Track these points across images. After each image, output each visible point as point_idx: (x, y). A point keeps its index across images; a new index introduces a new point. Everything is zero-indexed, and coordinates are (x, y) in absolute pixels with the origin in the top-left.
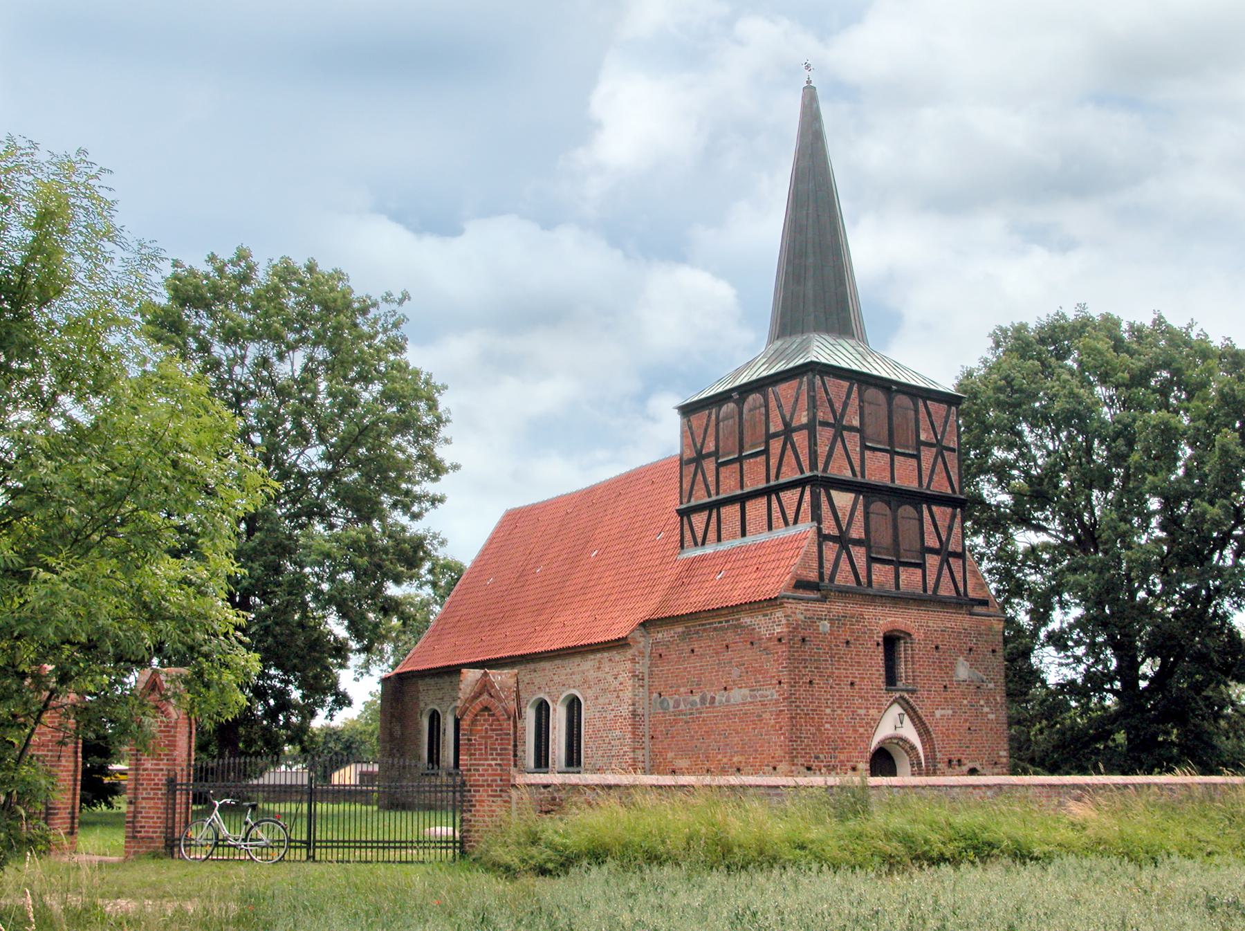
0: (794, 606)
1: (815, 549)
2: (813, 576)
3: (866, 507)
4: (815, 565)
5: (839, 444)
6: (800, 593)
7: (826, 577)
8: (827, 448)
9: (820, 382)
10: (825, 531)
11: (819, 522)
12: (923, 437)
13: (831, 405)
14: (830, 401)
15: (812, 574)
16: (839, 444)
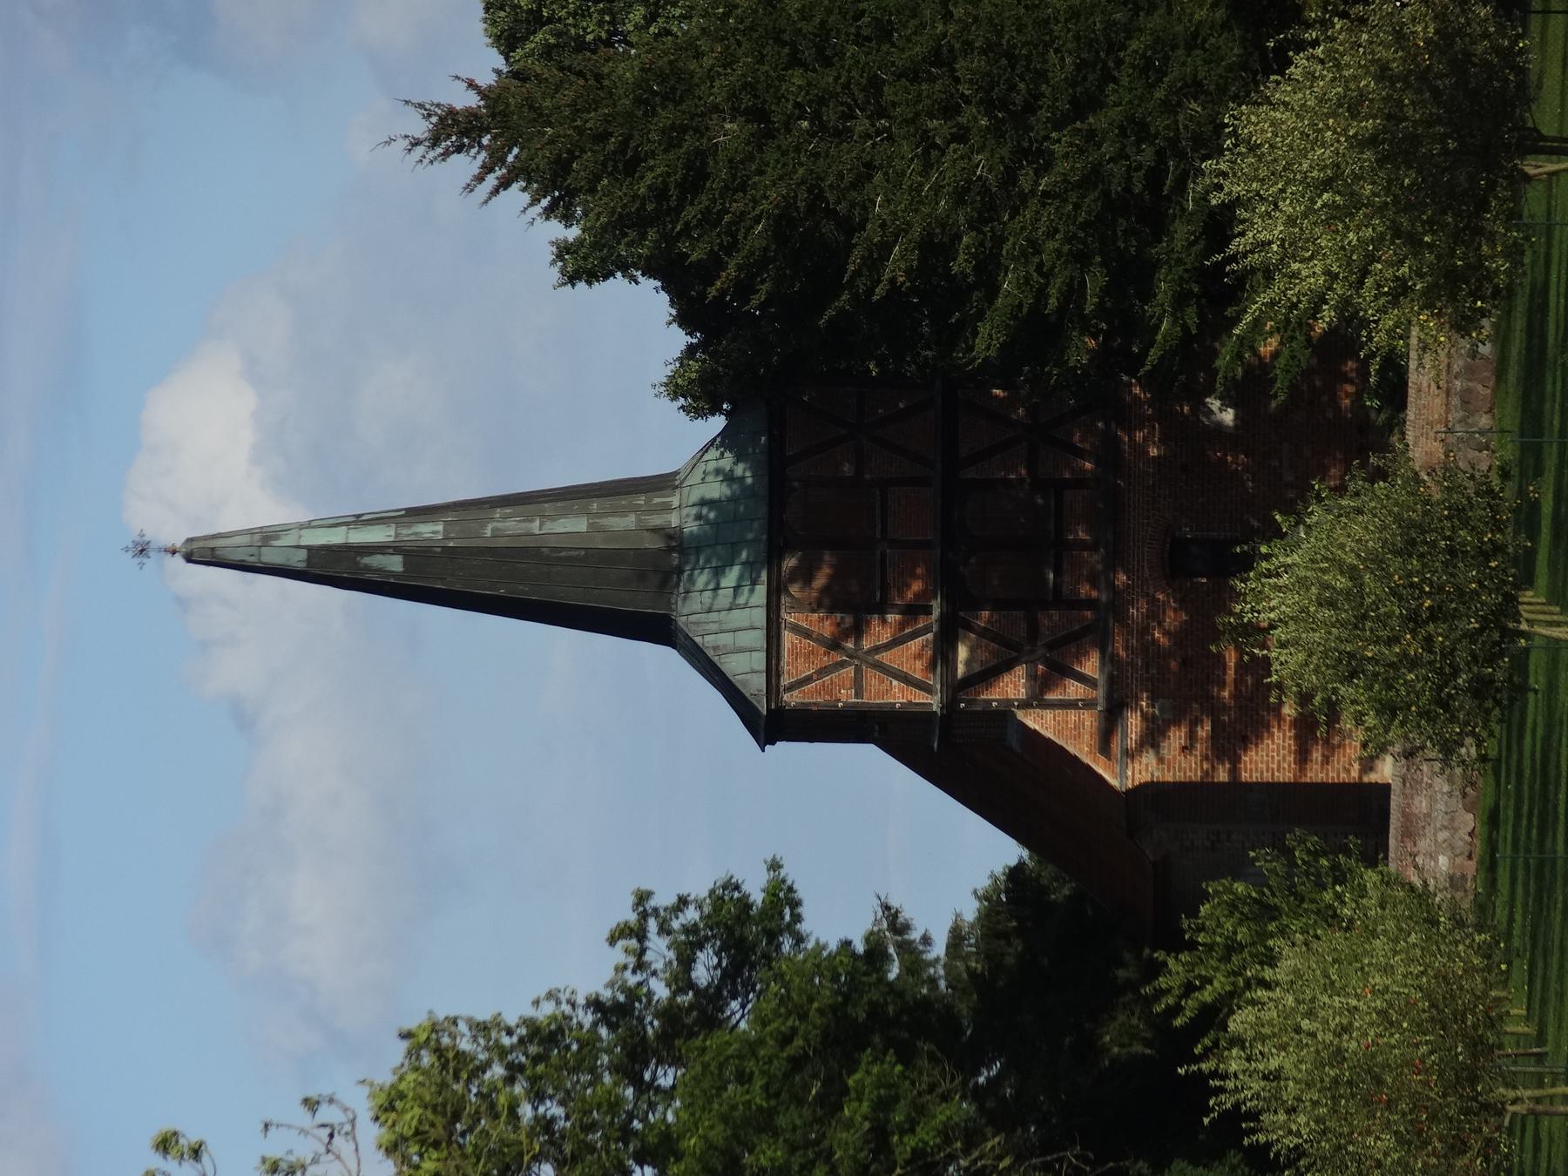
0: (1137, 771)
1: (1048, 714)
2: (1089, 720)
3: (976, 606)
4: (1072, 716)
5: (885, 657)
6: (1116, 746)
7: (1090, 693)
8: (895, 683)
9: (796, 693)
10: (1022, 693)
11: (1009, 702)
12: (847, 469)
13: (822, 672)
14: (822, 672)
15: (1087, 723)
16: (885, 657)
